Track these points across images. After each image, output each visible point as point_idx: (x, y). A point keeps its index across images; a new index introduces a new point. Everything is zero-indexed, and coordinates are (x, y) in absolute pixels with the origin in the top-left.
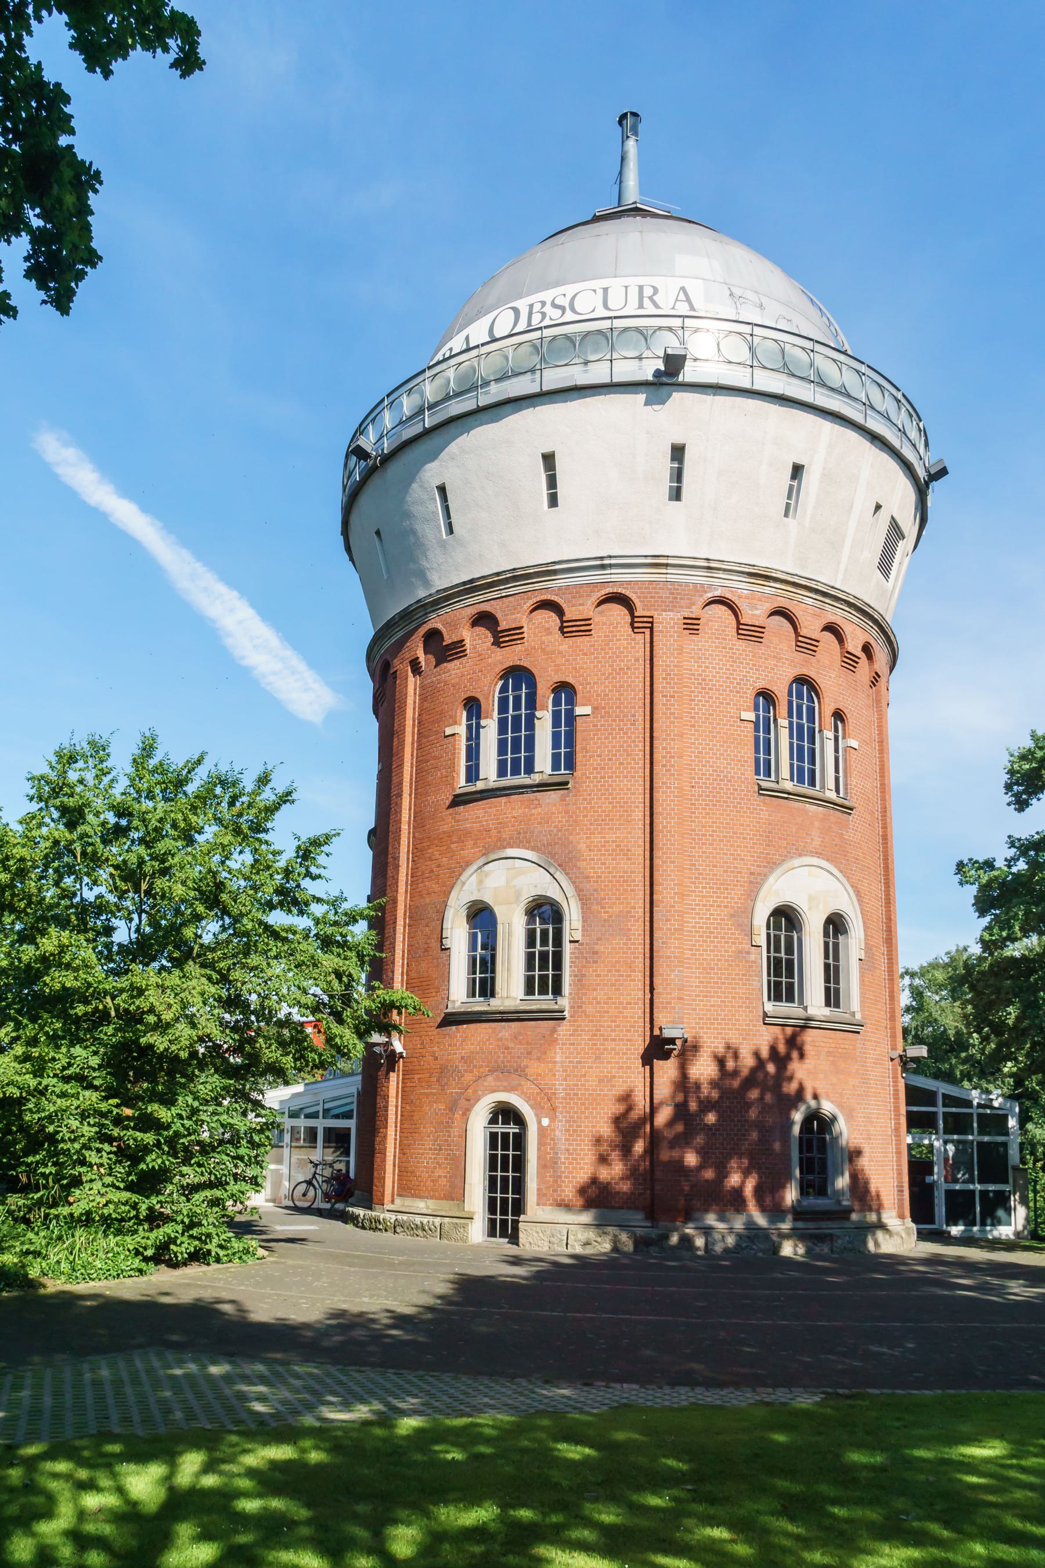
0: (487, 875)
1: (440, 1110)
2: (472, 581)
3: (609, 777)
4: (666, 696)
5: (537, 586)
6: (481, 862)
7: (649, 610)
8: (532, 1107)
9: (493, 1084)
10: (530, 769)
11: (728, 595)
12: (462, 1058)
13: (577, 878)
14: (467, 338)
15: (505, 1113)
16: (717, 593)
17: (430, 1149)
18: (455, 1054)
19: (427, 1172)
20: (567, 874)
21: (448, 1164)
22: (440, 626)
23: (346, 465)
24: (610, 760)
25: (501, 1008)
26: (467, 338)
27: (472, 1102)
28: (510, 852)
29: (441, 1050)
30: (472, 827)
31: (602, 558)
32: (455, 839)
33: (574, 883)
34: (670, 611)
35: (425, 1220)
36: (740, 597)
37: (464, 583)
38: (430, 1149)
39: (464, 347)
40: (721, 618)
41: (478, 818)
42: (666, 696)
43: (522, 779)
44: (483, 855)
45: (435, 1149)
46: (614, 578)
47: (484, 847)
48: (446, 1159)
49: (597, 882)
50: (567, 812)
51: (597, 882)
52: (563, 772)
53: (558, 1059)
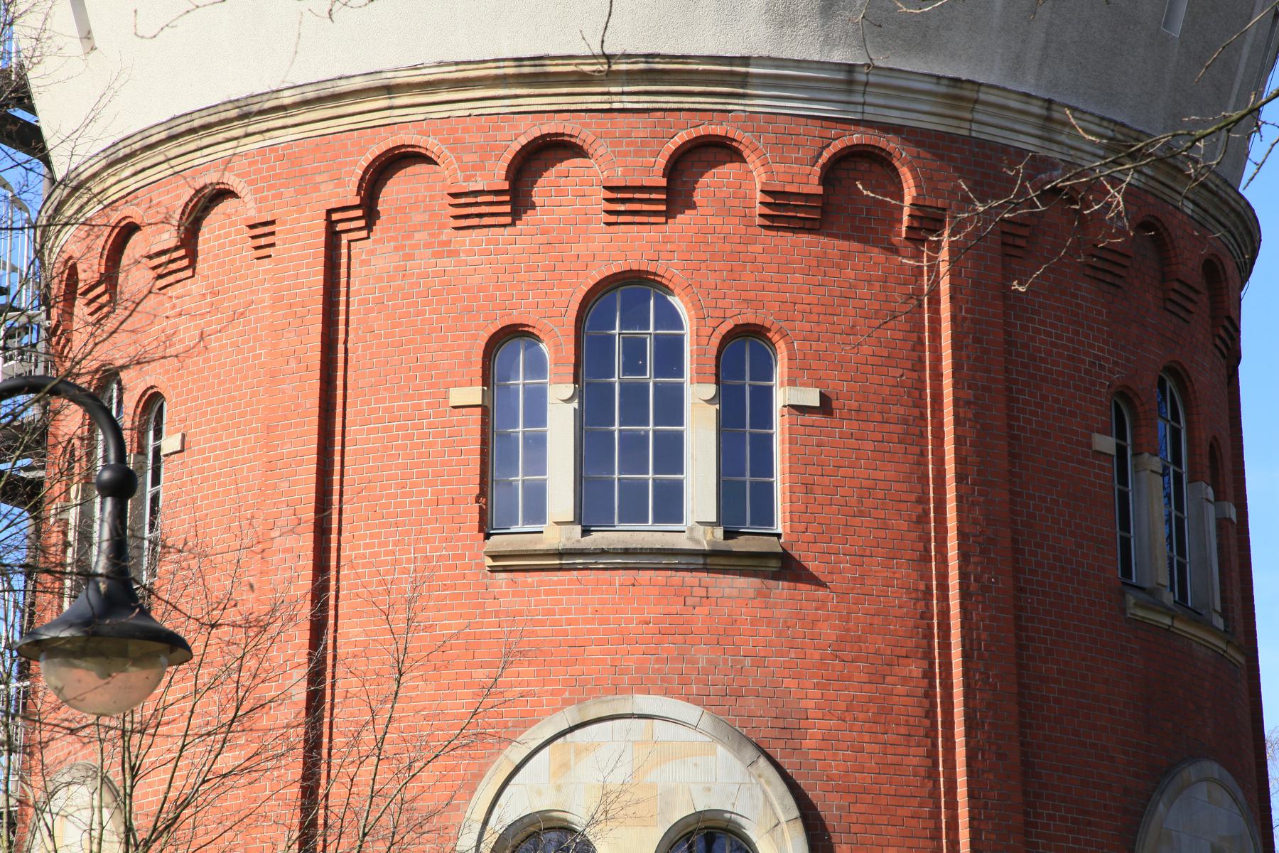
0: (580, 751)
28: (644, 703)
43: (649, 534)
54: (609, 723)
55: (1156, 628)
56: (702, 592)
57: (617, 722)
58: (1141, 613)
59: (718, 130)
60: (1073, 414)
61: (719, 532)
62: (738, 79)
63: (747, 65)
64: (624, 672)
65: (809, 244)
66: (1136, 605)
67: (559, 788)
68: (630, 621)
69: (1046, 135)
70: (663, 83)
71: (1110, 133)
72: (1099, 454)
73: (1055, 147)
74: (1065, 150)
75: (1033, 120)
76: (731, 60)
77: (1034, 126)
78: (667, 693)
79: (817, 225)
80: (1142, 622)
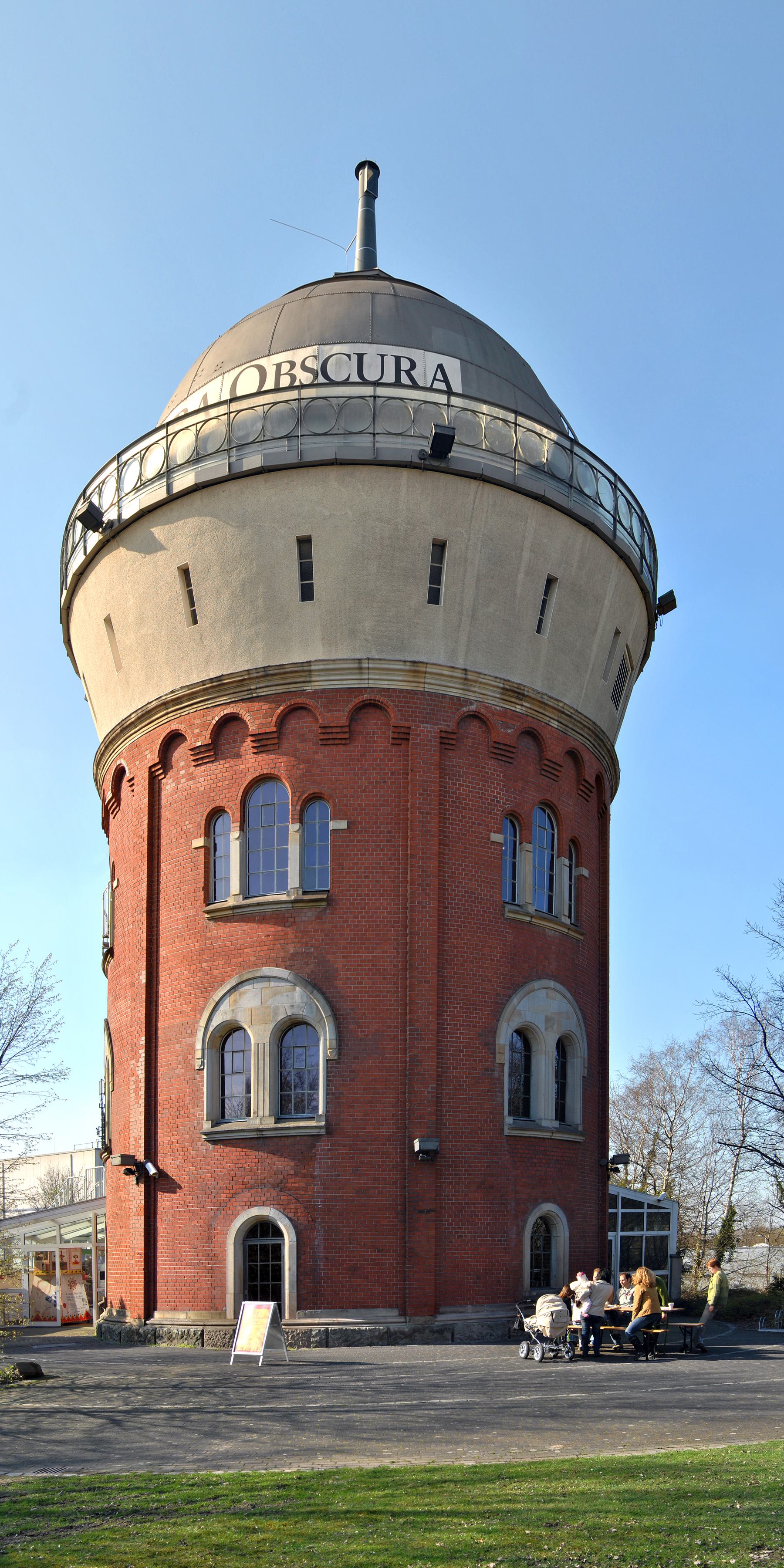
3: (366, 895)
4: (422, 813)
5: (293, 688)
6: (233, 982)
7: (407, 720)
10: (283, 885)
11: (483, 711)
14: (205, 398)
16: (473, 708)
24: (366, 877)
26: (205, 398)
32: (205, 957)
34: (427, 723)
36: (493, 714)
39: (202, 406)
40: (475, 734)
42: (422, 813)
46: (372, 683)
49: (354, 1001)
51: (354, 1001)
55: (522, 922)
58: (512, 915)
59: (299, 700)
60: (480, 824)
66: (509, 912)
69: (466, 687)
71: (501, 685)
72: (493, 843)
73: (471, 694)
74: (477, 695)
75: (458, 680)
77: (459, 683)
79: (348, 741)
80: (513, 920)
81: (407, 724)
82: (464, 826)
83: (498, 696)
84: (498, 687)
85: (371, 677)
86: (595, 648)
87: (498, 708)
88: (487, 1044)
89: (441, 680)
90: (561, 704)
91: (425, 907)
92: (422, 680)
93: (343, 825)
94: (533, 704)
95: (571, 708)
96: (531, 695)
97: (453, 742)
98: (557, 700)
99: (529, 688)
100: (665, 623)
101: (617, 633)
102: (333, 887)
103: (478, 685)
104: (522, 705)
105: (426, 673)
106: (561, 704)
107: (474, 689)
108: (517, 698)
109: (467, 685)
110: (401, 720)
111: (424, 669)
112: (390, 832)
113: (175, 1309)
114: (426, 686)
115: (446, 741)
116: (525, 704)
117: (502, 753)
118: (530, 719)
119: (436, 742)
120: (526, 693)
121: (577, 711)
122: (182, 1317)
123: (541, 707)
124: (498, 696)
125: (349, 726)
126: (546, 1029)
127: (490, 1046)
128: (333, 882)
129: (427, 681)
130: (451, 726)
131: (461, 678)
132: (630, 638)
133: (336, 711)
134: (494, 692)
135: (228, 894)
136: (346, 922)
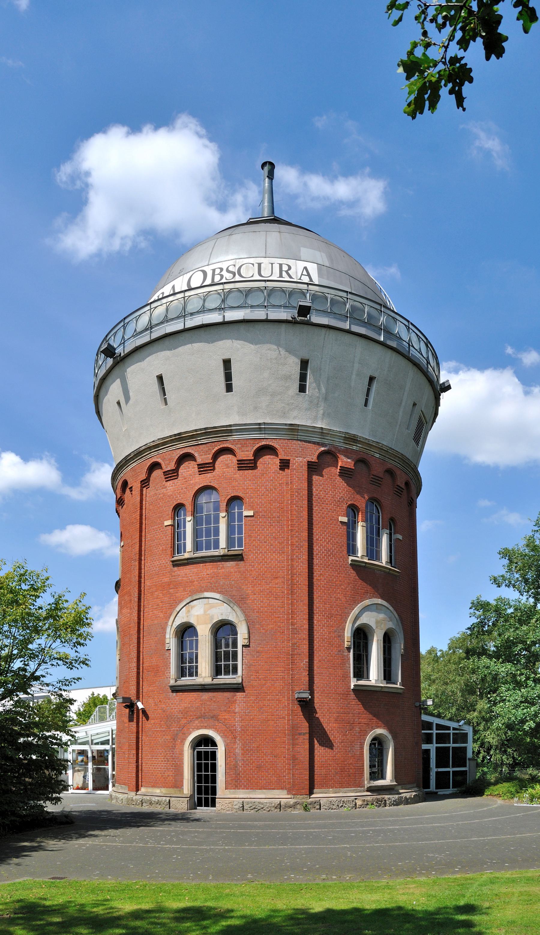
0: (192, 607)
1: (167, 740)
2: (179, 434)
4: (298, 507)
7: (287, 456)
8: (221, 737)
9: (199, 725)
11: (333, 449)
12: (180, 711)
13: (246, 609)
15: (207, 741)
17: (162, 761)
18: (175, 709)
19: (161, 773)
20: (240, 607)
21: (173, 769)
22: (159, 460)
23: (97, 361)
24: (265, 542)
25: (203, 683)
27: (186, 735)
29: (167, 707)
30: (182, 580)
31: (260, 424)
33: (244, 612)
35: (160, 799)
37: (175, 435)
38: (162, 761)
41: (186, 574)
44: (189, 596)
45: (165, 761)
47: (190, 591)
48: (172, 766)
50: (239, 572)
52: (236, 549)
53: (237, 710)
54: (198, 600)
56: (222, 566)
57: (200, 600)
59: (225, 445)
61: (226, 550)
62: (229, 431)
63: (231, 427)
64: (203, 587)
65: (251, 473)
67: (187, 616)
68: (204, 575)
69: (322, 437)
70: (209, 435)
71: (344, 435)
73: (326, 440)
74: (329, 441)
76: (227, 426)
77: (318, 435)
78: (214, 592)
79: (254, 468)
81: (288, 458)
82: (323, 513)
83: (342, 441)
84: (341, 436)
85: (266, 432)
86: (401, 413)
87: (343, 448)
88: (339, 636)
89: (308, 433)
90: (380, 445)
91: (300, 559)
92: (296, 434)
93: (251, 513)
94: (363, 445)
95: (387, 446)
96: (362, 440)
97: (316, 467)
98: (377, 442)
99: (360, 436)
100: (445, 397)
101: (415, 404)
102: (245, 548)
103: (330, 435)
104: (356, 446)
105: (298, 430)
106: (380, 445)
107: (327, 438)
108: (354, 442)
109: (323, 436)
110: (284, 455)
111: (297, 428)
112: (278, 517)
113: (153, 786)
114: (299, 437)
115: (312, 467)
116: (358, 445)
117: (345, 472)
118: (361, 453)
119: (305, 468)
120: (359, 439)
121: (390, 448)
122: (157, 791)
123: (369, 447)
124: (342, 441)
125: (254, 460)
126: (377, 627)
127: (341, 636)
128: (245, 546)
129: (299, 434)
130: (314, 459)
131: (319, 432)
132: (423, 407)
133: (247, 451)
134: (339, 439)
135: (185, 552)
136: (254, 567)
